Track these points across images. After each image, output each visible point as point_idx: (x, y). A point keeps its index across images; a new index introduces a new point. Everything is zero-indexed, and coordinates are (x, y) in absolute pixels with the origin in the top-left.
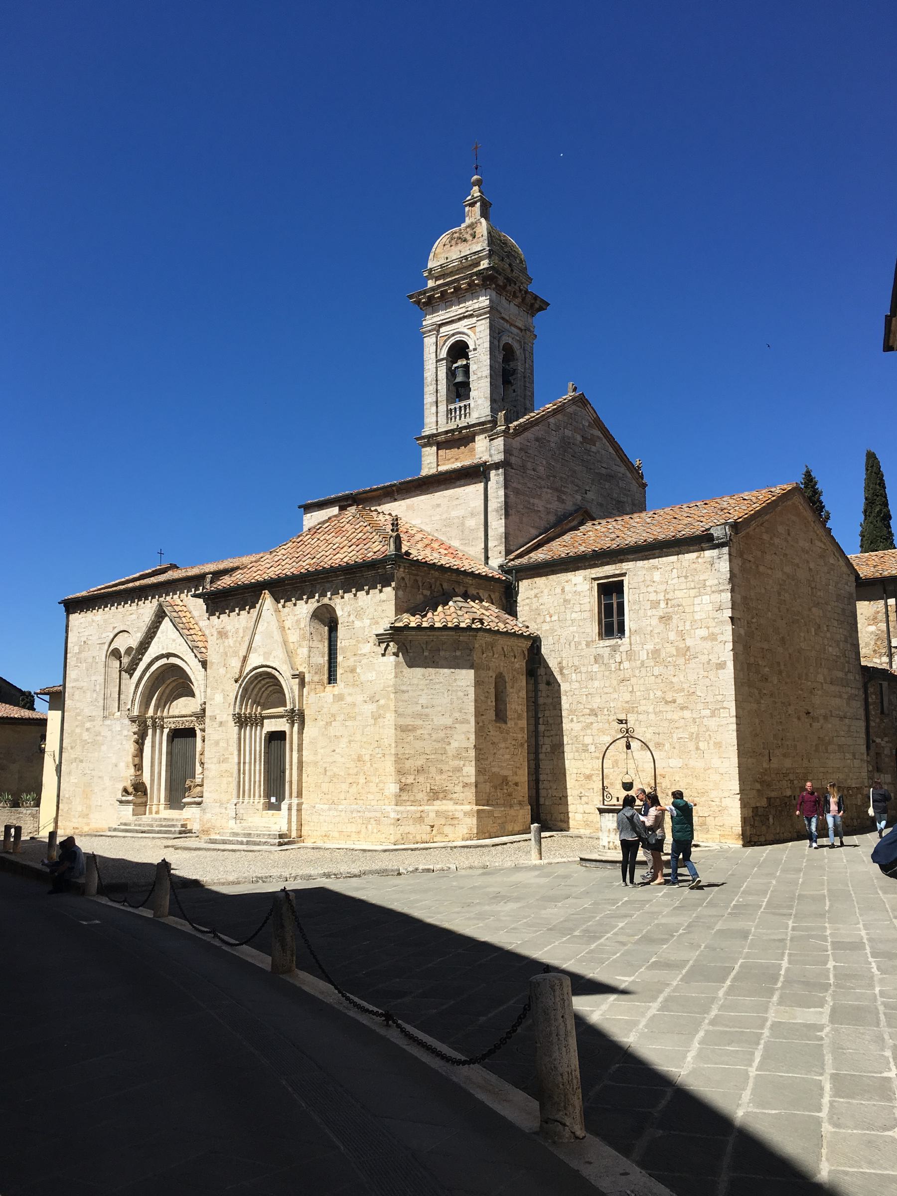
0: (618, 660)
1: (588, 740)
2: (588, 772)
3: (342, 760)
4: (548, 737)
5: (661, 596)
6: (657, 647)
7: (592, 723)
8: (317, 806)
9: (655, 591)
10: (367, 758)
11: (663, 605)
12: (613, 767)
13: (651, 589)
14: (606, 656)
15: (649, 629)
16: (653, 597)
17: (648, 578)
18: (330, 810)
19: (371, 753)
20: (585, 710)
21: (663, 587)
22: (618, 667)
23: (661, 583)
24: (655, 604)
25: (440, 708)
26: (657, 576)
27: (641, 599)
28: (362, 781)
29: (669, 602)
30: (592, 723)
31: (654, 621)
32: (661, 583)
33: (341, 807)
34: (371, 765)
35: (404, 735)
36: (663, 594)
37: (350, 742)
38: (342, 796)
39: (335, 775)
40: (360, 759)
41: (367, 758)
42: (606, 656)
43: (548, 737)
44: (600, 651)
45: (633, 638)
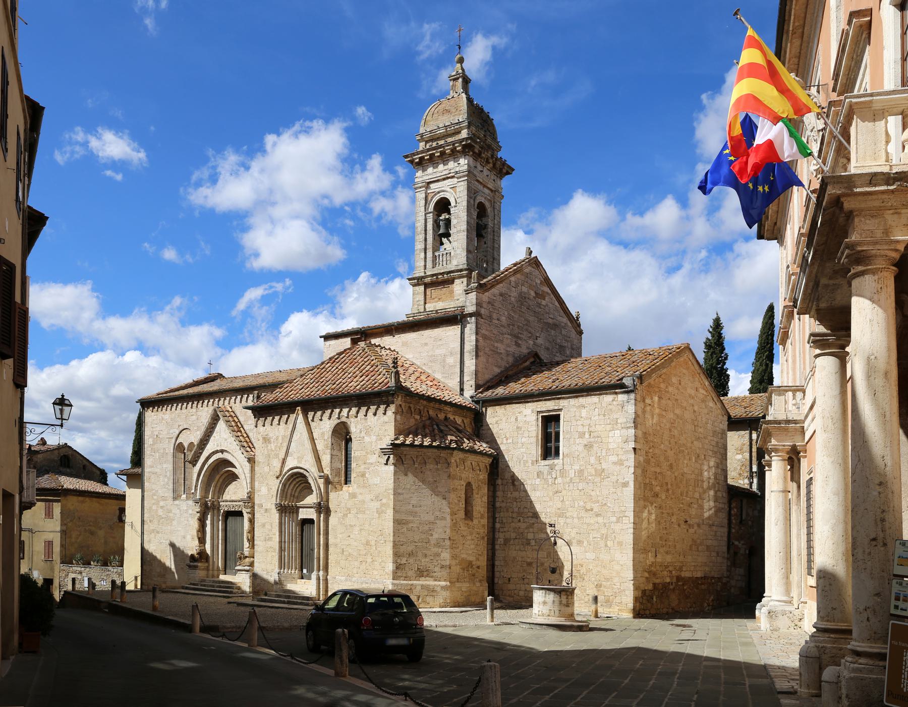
0: (554, 476)
1: (530, 536)
2: (529, 560)
3: (355, 544)
4: (502, 532)
5: (586, 429)
6: (582, 468)
7: (533, 524)
8: (337, 577)
9: (582, 425)
10: (373, 543)
11: (587, 436)
12: (547, 558)
13: (579, 423)
14: (546, 472)
15: (577, 453)
16: (580, 429)
17: (577, 414)
18: (346, 580)
19: (376, 539)
20: (529, 514)
21: (588, 422)
22: (553, 482)
23: (587, 418)
24: (582, 435)
25: (425, 508)
26: (584, 413)
27: (572, 430)
28: (369, 560)
29: (592, 434)
30: (533, 524)
31: (581, 448)
32: (587, 418)
33: (354, 579)
34: (376, 549)
35: (400, 527)
36: (587, 427)
37: (361, 530)
38: (355, 571)
39: (350, 555)
40: (368, 543)
41: (373, 543)
42: (546, 472)
43: (502, 532)
44: (542, 469)
45: (565, 460)
